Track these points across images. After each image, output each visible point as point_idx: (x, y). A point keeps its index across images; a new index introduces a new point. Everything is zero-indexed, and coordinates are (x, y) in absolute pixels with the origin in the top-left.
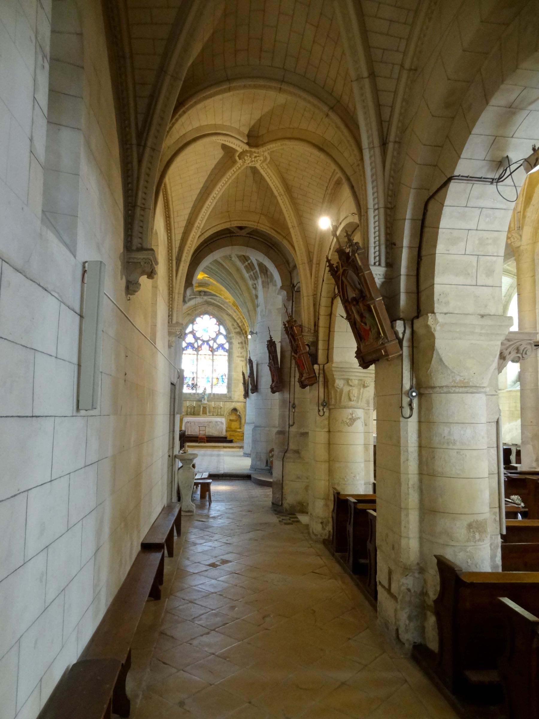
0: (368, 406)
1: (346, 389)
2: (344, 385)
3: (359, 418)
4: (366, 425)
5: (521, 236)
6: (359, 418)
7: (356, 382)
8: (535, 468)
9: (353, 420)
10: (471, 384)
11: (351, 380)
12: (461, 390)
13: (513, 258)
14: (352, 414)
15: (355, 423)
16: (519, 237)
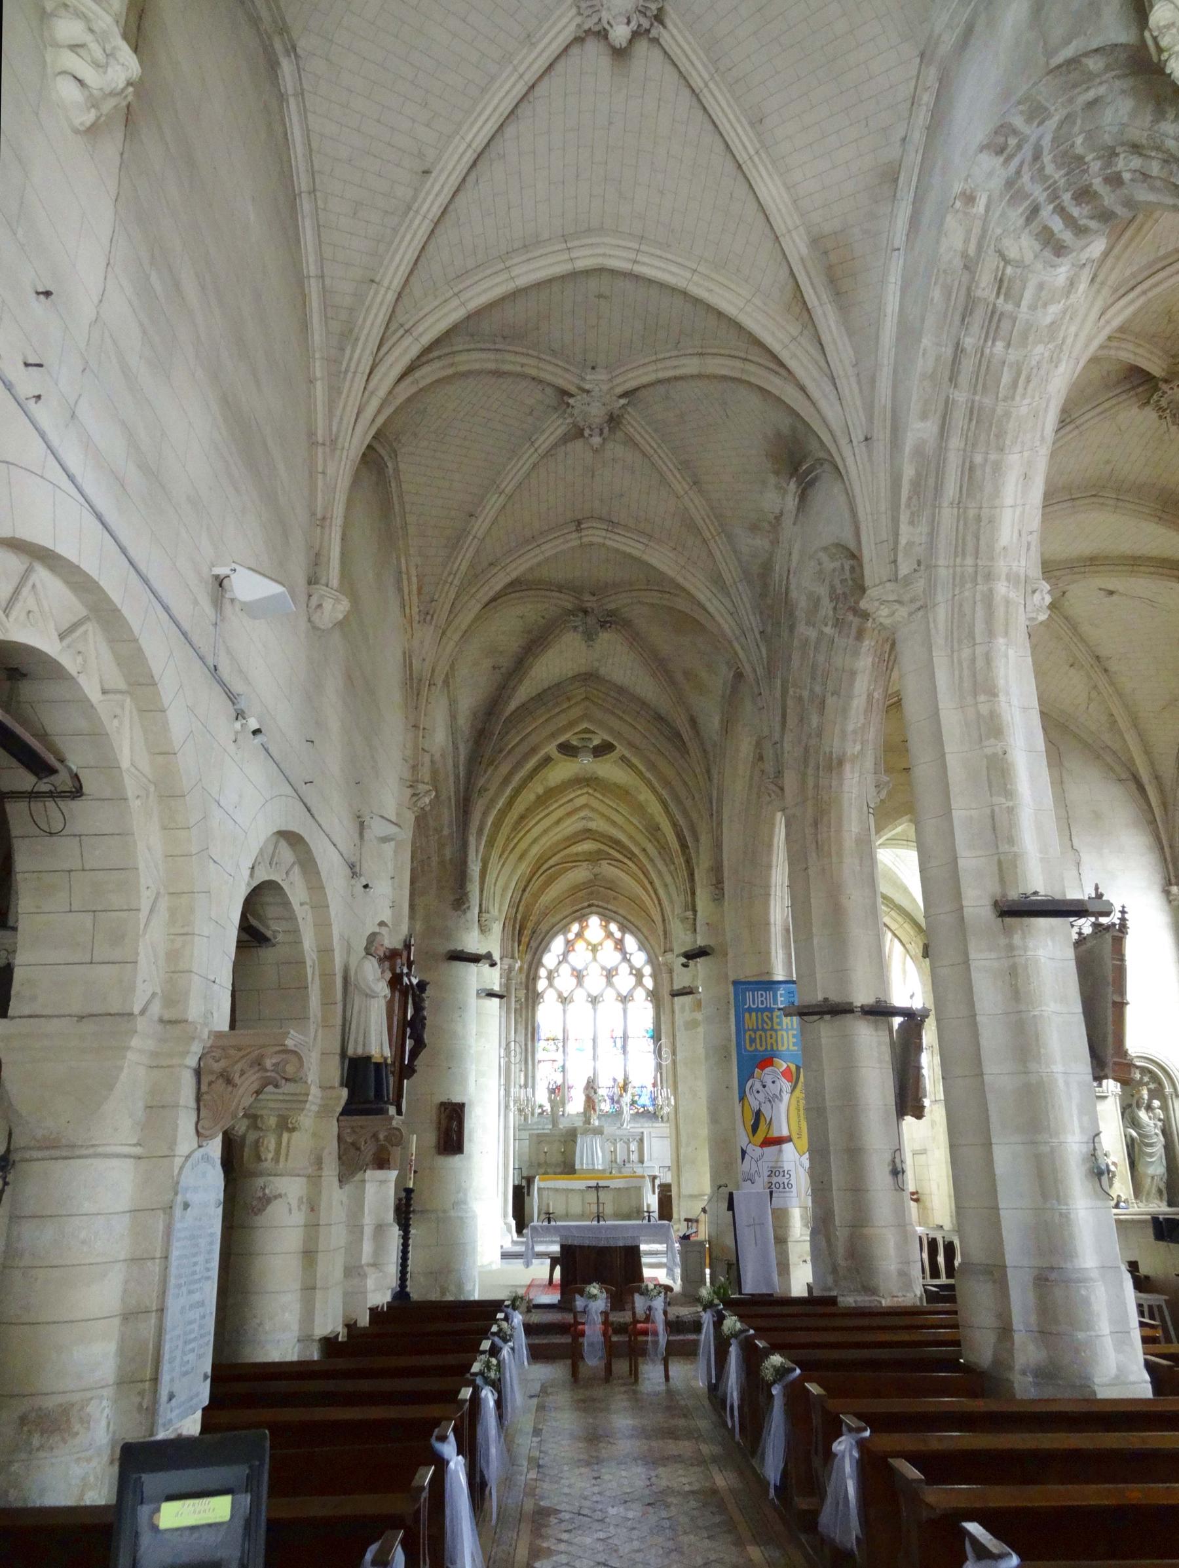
0: (320, 1169)
1: (252, 1137)
2: (248, 1128)
3: (280, 1196)
4: (312, 1210)
5: (782, 789)
6: (280, 1196)
7: (272, 1121)
8: (830, 1289)
9: (266, 1201)
10: (64, 1141)
11: (262, 1116)
12: (39, 1154)
13: (907, 817)
14: (263, 1189)
15: (270, 1209)
16: (777, 790)
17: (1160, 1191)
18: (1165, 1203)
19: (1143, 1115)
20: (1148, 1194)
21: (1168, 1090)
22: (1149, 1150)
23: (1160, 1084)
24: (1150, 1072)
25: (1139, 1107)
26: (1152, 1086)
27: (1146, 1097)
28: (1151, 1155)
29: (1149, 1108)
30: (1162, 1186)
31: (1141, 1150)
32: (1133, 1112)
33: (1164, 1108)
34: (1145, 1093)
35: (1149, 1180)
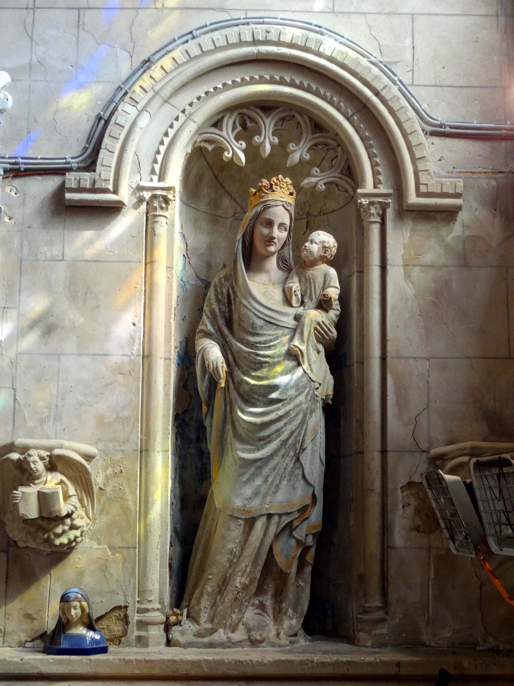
17: (270, 575)
18: (292, 622)
19: (264, 288)
20: (224, 583)
21: (371, 183)
22: (248, 415)
23: (351, 172)
24: (319, 125)
25: (252, 256)
26: (317, 180)
27: (282, 215)
28: (256, 435)
29: (296, 263)
30: (286, 554)
31: (229, 417)
32: (232, 276)
33: (348, 260)
34: (281, 201)
35: (236, 532)
